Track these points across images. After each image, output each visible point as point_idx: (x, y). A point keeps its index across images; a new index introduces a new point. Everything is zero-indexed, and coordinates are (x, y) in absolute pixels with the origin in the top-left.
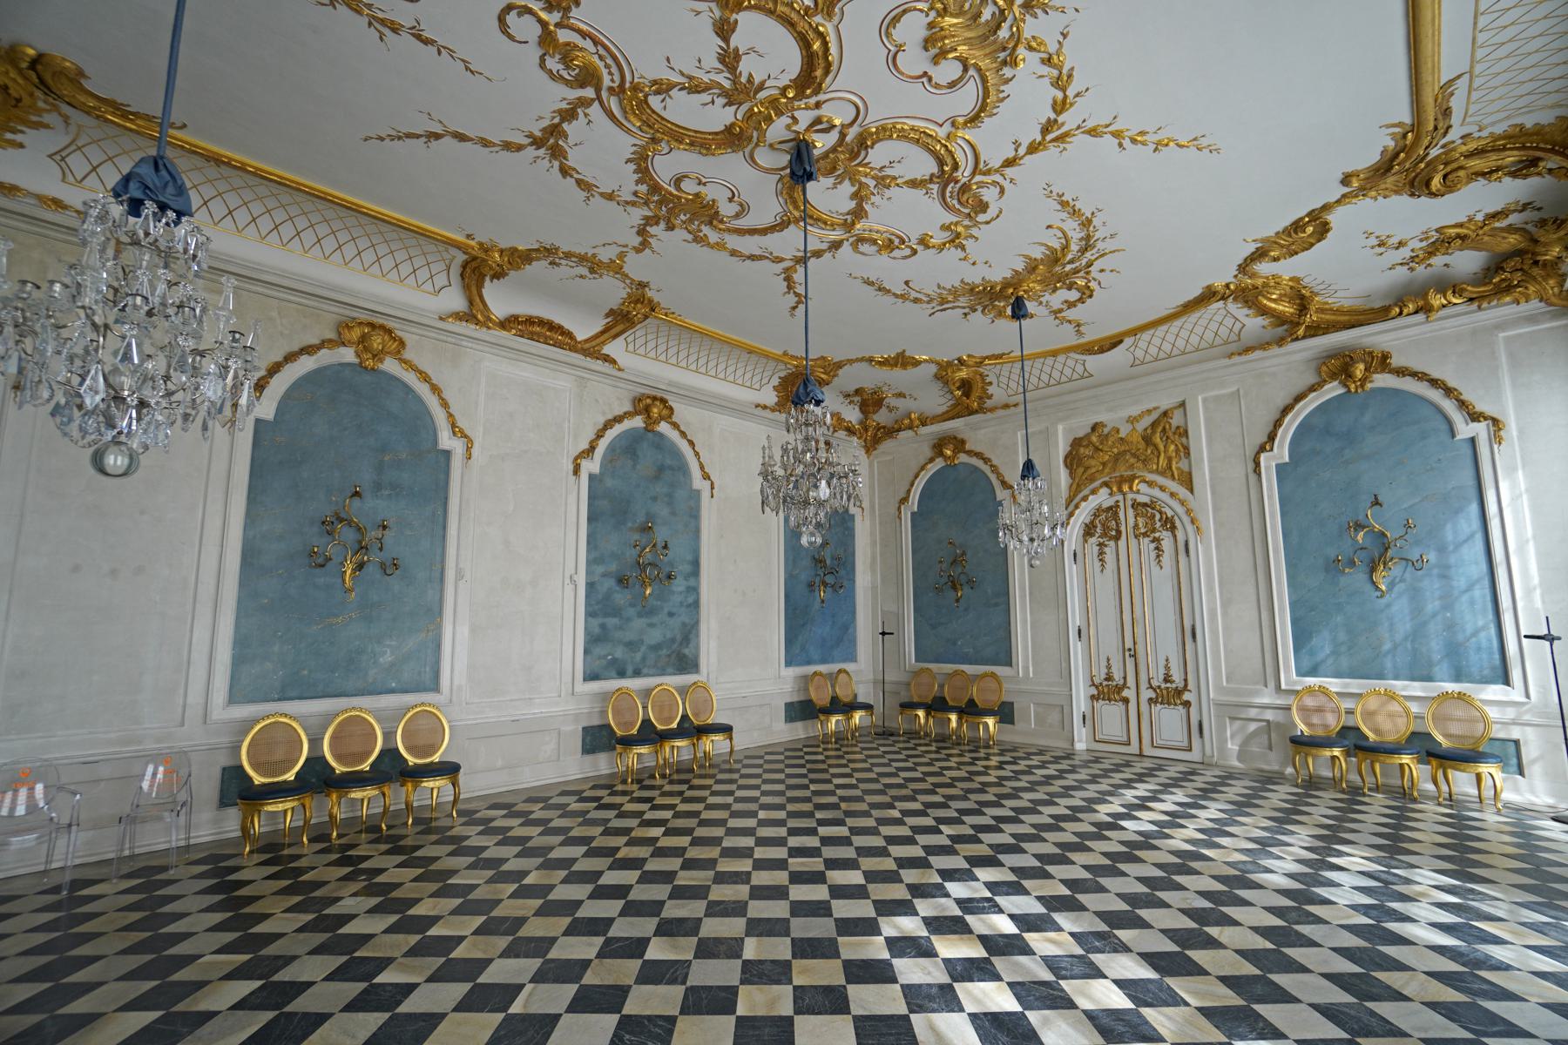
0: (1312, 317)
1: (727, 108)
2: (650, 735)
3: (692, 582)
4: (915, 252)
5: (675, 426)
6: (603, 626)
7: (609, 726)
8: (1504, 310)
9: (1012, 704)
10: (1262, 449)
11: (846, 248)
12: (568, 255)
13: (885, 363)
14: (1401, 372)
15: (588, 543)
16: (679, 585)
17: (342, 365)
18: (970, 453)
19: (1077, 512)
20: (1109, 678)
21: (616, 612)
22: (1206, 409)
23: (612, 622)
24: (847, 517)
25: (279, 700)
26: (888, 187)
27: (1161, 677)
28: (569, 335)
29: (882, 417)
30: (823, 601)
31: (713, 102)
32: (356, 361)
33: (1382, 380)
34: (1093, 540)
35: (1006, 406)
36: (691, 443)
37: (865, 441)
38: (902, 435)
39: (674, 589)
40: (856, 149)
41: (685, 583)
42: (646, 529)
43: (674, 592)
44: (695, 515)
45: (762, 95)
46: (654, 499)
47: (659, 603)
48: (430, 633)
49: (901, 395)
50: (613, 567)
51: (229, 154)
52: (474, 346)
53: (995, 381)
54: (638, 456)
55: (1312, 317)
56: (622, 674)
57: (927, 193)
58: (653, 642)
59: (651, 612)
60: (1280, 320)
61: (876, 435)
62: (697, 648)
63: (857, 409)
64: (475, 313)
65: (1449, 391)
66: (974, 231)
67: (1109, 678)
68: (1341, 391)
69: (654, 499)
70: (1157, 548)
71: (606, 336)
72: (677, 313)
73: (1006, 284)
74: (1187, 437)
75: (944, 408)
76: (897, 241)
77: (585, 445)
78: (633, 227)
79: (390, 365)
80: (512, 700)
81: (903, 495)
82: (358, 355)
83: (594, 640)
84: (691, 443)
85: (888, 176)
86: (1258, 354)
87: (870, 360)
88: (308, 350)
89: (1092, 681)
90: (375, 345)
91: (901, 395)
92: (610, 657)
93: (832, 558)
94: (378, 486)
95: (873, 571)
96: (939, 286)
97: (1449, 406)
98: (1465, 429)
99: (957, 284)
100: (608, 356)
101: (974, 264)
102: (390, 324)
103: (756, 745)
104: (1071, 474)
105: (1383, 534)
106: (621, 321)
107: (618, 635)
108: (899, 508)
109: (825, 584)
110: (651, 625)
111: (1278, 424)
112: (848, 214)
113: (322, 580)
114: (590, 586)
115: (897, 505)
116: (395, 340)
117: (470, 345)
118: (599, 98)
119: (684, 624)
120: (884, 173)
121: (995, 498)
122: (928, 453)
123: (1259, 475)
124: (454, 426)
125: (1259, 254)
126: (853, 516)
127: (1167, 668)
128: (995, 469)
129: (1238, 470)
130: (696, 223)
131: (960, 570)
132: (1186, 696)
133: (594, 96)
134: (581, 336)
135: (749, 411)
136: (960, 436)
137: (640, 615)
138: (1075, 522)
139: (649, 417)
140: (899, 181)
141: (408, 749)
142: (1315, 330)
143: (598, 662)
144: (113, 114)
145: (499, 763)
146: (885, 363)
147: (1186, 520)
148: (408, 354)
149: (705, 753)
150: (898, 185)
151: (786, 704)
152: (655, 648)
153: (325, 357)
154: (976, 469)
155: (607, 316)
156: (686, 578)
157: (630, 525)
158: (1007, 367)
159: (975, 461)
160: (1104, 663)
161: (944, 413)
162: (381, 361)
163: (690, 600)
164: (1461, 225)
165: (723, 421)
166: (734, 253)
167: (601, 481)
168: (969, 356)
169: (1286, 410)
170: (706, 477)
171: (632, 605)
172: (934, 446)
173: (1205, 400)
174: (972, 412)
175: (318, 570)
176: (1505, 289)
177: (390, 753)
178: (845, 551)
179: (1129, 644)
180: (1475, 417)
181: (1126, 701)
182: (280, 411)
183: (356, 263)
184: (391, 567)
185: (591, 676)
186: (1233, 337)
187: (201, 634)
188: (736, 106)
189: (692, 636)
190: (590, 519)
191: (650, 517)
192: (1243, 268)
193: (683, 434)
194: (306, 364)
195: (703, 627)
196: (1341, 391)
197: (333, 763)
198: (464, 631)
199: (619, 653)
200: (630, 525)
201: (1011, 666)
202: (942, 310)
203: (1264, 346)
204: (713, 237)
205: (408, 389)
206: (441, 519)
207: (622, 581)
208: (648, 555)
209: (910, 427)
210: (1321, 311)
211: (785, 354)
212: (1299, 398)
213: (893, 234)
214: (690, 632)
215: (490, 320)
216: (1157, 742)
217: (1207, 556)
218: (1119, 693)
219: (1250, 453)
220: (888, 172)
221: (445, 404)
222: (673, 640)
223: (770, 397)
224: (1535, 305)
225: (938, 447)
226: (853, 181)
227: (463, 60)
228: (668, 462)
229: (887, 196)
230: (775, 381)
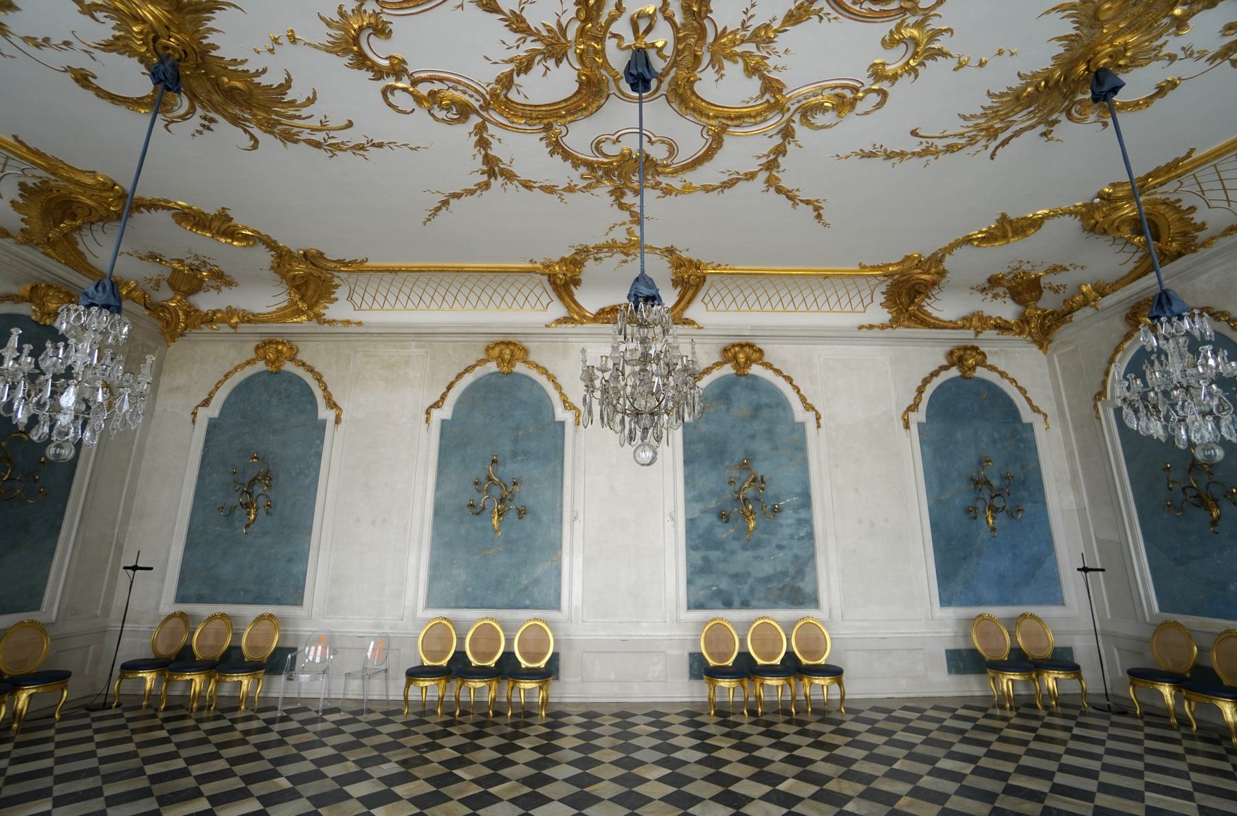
1: (561, 65)
2: (745, 669)
3: (803, 514)
4: (883, 94)
5: (768, 366)
6: (706, 559)
7: (701, 654)
11: (800, 131)
12: (599, 248)
13: (990, 238)
15: (686, 483)
16: (788, 518)
21: (719, 545)
23: (714, 555)
24: (1019, 426)
25: (455, 607)
26: (771, 41)
30: (993, 529)
31: (547, 68)
36: (789, 379)
37: (1030, 334)
38: (1078, 316)
39: (782, 521)
40: (695, 24)
41: (795, 515)
42: (744, 466)
43: (781, 525)
44: (800, 447)
45: (571, 34)
46: (753, 437)
47: (765, 536)
48: (554, 563)
49: (1055, 270)
50: (713, 504)
51: (392, 265)
52: (577, 339)
53: (1198, 202)
54: (731, 400)
56: (728, 605)
57: (821, 18)
58: (761, 575)
59: (758, 545)
61: (1042, 324)
62: (815, 581)
63: (1009, 302)
64: (575, 316)
66: (934, 24)
69: (753, 437)
71: (683, 304)
72: (722, 263)
73: (1067, 63)
75: (1131, 266)
76: (848, 94)
78: (612, 205)
79: (520, 368)
80: (621, 622)
81: (1098, 389)
82: (498, 366)
83: (696, 572)
84: (789, 379)
85: (759, 28)
87: (968, 240)
88: (468, 370)
90: (506, 356)
91: (1055, 270)
92: (714, 588)
93: (1004, 477)
94: (514, 454)
95: (1076, 488)
96: (964, 118)
99: (988, 102)
100: (687, 319)
101: (981, 64)
103: (905, 696)
107: (722, 566)
108: (1095, 406)
109: (995, 510)
110: (757, 558)
112: (763, 94)
113: (480, 523)
114: (691, 523)
115: (1092, 403)
116: (521, 350)
117: (574, 339)
118: (485, 119)
119: (796, 557)
120: (751, 29)
124: (565, 402)
126: (1031, 424)
130: (649, 177)
133: (481, 120)
137: (745, 548)
140: (776, 25)
141: (522, 654)
143: (702, 592)
144: (344, 267)
145: (612, 677)
146: (990, 238)
148: (532, 358)
149: (806, 696)
150: (777, 31)
151: (948, 652)
152: (767, 580)
153: (479, 372)
156: (795, 511)
158: (1188, 181)
161: (1131, 272)
165: (825, 352)
166: (707, 189)
167: (695, 427)
168: (1113, 185)
170: (809, 407)
171: (735, 539)
172: (1127, 318)
175: (477, 517)
177: (509, 656)
178: (1023, 467)
182: (455, 412)
183: (503, 305)
184: (521, 513)
185: (695, 605)
187: (412, 561)
188: (565, 58)
189: (807, 569)
190: (687, 462)
194: (469, 379)
195: (820, 560)
197: (471, 658)
198: (579, 562)
199: (724, 584)
200: (727, 463)
202: (1003, 144)
204: (676, 183)
205: (533, 382)
206: (559, 474)
207: (724, 517)
208: (750, 492)
209: (1085, 303)
213: (836, 87)
214: (805, 563)
215: (585, 317)
220: (754, 24)
221: (558, 387)
222: (785, 574)
223: (884, 316)
226: (732, 57)
227: (404, 145)
228: (765, 400)
229: (781, 50)
230: (881, 299)
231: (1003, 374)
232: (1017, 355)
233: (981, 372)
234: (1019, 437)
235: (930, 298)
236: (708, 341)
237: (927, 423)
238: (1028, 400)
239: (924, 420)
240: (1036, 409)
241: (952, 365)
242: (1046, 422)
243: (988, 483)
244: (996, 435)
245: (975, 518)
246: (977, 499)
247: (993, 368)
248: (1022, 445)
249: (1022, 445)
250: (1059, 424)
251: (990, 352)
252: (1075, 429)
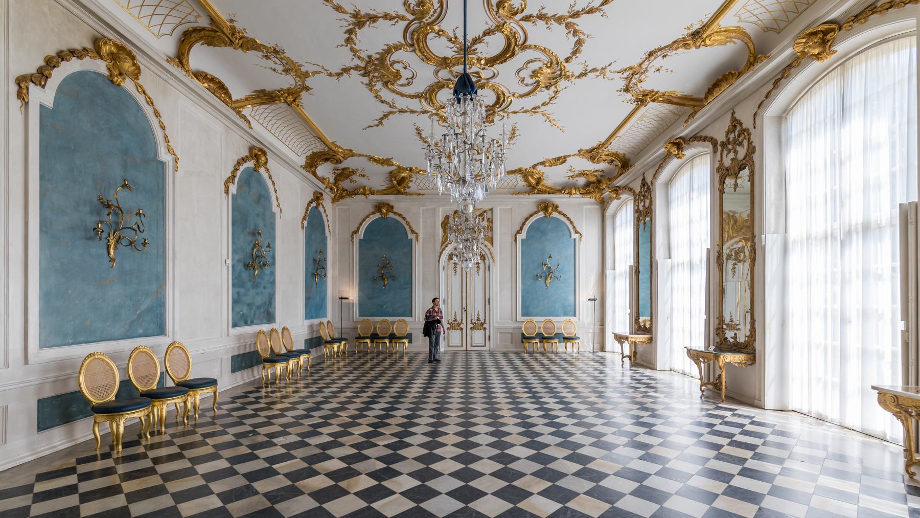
0: (540, 187)
8: (587, 199)
9: (411, 334)
10: (518, 232)
14: (560, 213)
16: (267, 270)
17: (96, 73)
18: (395, 213)
19: (446, 248)
20: (455, 320)
22: (500, 213)
27: (476, 319)
28: (227, 93)
29: (345, 184)
32: (106, 73)
33: (555, 215)
34: (451, 262)
35: (419, 194)
38: (358, 197)
53: (414, 181)
55: (540, 187)
60: (530, 185)
62: (275, 308)
65: (571, 222)
67: (455, 320)
68: (543, 216)
70: (478, 267)
74: (492, 223)
75: (383, 188)
77: (229, 175)
81: (354, 229)
86: (522, 196)
89: (448, 321)
97: (571, 227)
98: (574, 236)
102: (135, 52)
104: (444, 231)
105: (550, 267)
106: (265, 97)
108: (352, 236)
111: (524, 224)
121: (407, 237)
122: (371, 210)
123: (516, 242)
125: (543, 163)
127: (478, 315)
128: (408, 223)
129: (509, 239)
132: (485, 326)
134: (234, 98)
135: (296, 167)
136: (391, 204)
138: (445, 253)
139: (257, 161)
142: (540, 192)
147: (490, 256)
154: (398, 222)
155: (255, 91)
157: (248, 230)
159: (397, 218)
160: (453, 314)
161: (382, 190)
162: (124, 79)
163: (272, 280)
164: (589, 171)
168: (416, 168)
169: (527, 219)
173: (500, 210)
174: (399, 193)
176: (588, 193)
179: (464, 306)
180: (576, 232)
181: (462, 329)
186: (513, 187)
191: (256, 226)
192: (534, 166)
193: (270, 177)
196: (543, 216)
201: (412, 316)
203: (524, 193)
205: (139, 108)
209: (364, 194)
210: (543, 185)
211: (333, 143)
212: (531, 216)
214: (270, 301)
216: (473, 344)
217: (496, 270)
218: (459, 326)
219: (514, 233)
223: (302, 161)
224: (593, 200)
225: (378, 207)
230: (308, 154)
236: (245, 137)
252: (339, 243)
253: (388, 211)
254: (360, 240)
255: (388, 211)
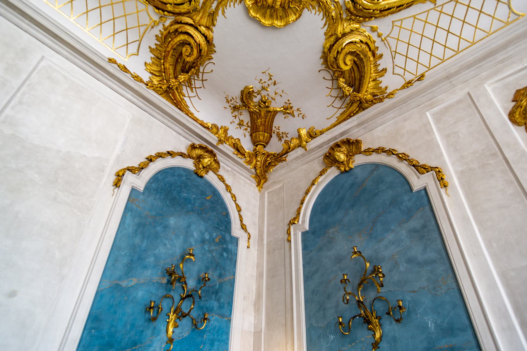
18: (368, 152)
24: (228, 237)
38: (291, 156)
61: (266, 161)
93: (203, 281)
95: (257, 310)
108: (289, 229)
109: (181, 315)
115: (286, 228)
121: (411, 190)
128: (403, 157)
131: (372, 295)
136: (353, 138)
154: (377, 166)
159: (375, 158)
178: (220, 276)
231: (228, 188)
232: (242, 181)
233: (211, 177)
234: (225, 246)
235: (192, 92)
237: (143, 193)
238: (240, 216)
239: (142, 188)
240: (244, 227)
241: (190, 157)
242: (248, 242)
243: (181, 279)
244: (207, 237)
245: (154, 319)
246: (166, 297)
247: (222, 179)
248: (225, 255)
249: (225, 255)
250: (257, 248)
251: (224, 168)
252: (268, 252)
253: (349, 156)
254: (304, 234)
255: (349, 156)
